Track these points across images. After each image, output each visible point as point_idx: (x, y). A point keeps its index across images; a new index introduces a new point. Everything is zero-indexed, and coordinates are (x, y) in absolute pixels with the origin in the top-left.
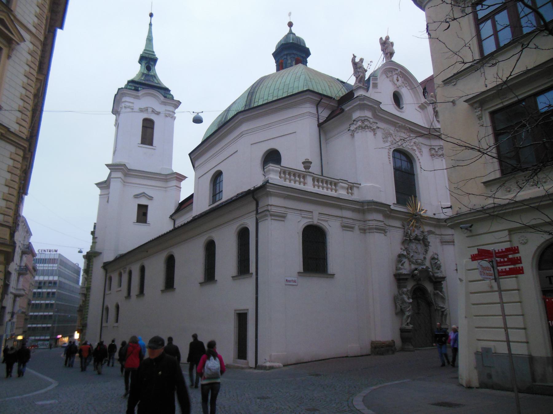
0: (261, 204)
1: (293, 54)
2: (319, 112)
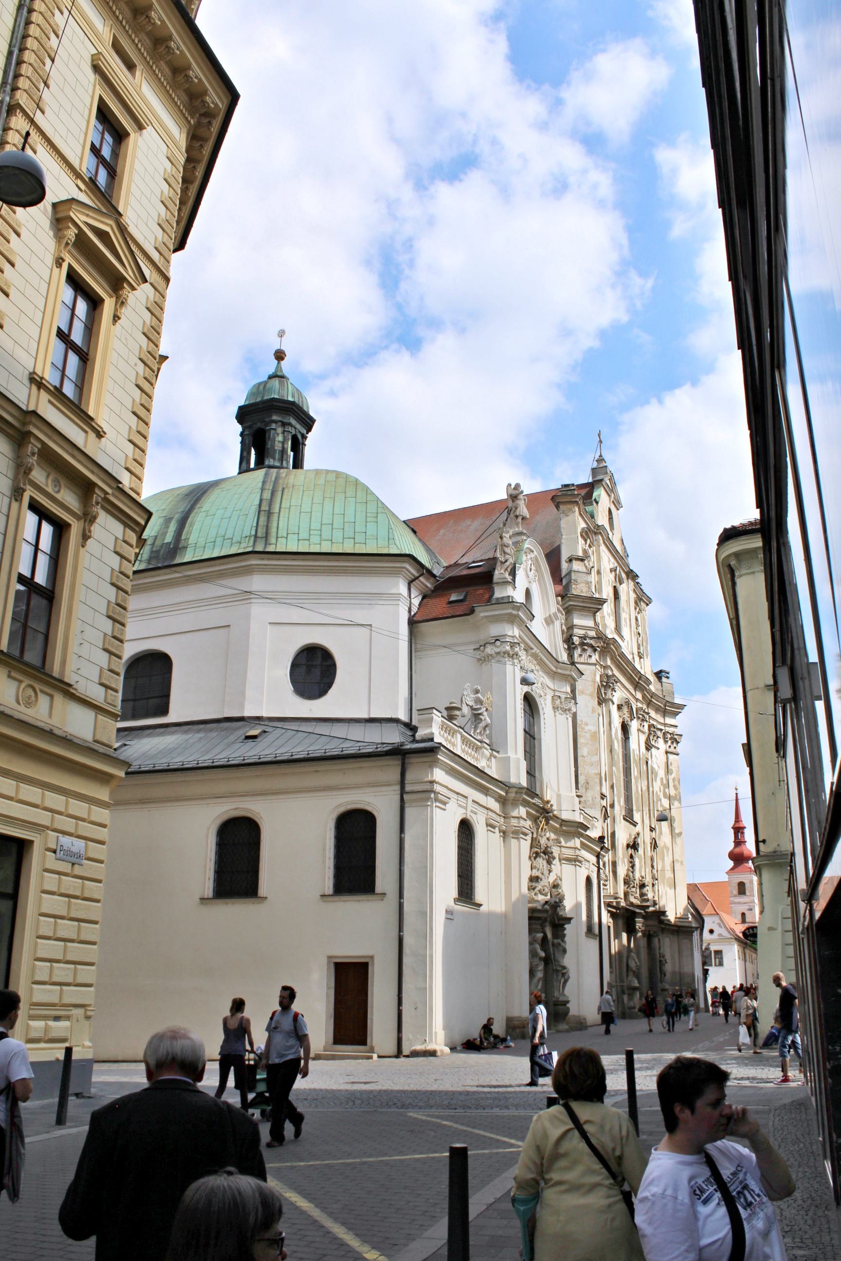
0: (409, 777)
1: (290, 424)
2: (413, 596)
